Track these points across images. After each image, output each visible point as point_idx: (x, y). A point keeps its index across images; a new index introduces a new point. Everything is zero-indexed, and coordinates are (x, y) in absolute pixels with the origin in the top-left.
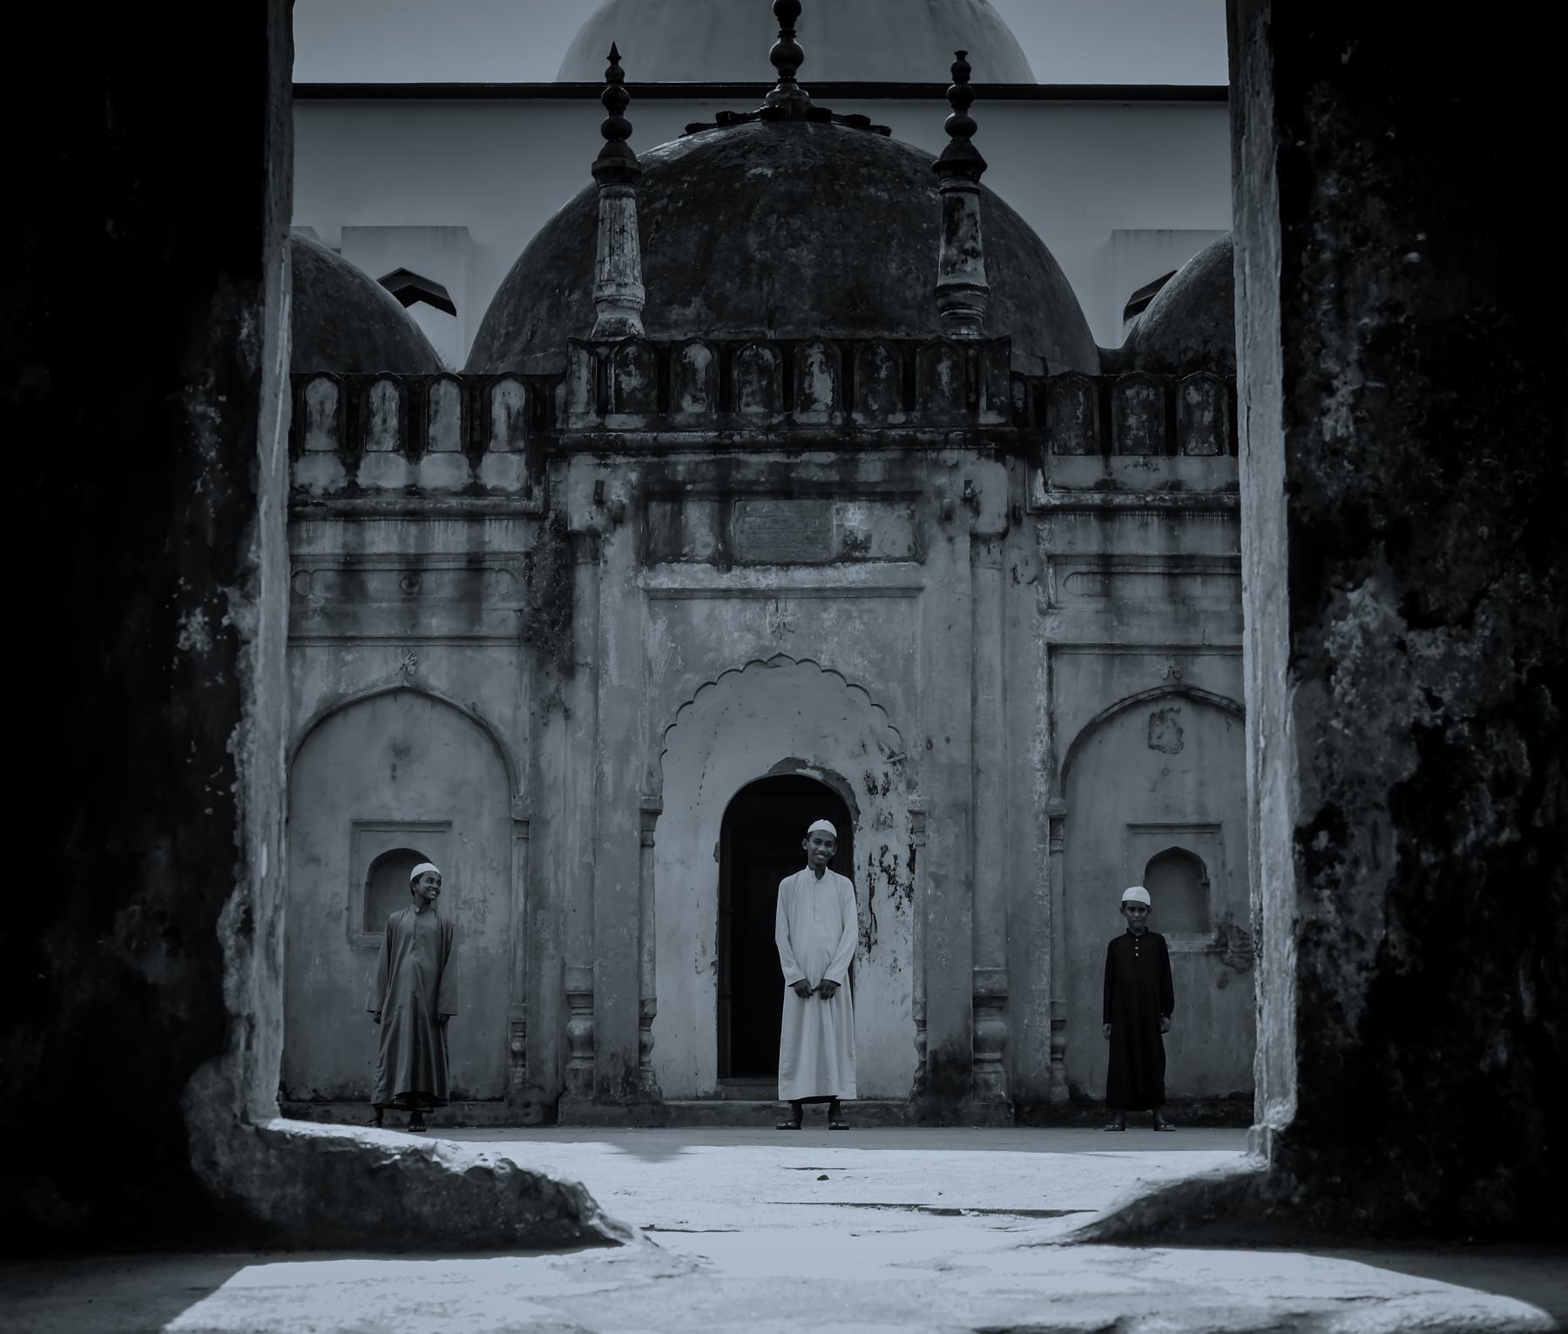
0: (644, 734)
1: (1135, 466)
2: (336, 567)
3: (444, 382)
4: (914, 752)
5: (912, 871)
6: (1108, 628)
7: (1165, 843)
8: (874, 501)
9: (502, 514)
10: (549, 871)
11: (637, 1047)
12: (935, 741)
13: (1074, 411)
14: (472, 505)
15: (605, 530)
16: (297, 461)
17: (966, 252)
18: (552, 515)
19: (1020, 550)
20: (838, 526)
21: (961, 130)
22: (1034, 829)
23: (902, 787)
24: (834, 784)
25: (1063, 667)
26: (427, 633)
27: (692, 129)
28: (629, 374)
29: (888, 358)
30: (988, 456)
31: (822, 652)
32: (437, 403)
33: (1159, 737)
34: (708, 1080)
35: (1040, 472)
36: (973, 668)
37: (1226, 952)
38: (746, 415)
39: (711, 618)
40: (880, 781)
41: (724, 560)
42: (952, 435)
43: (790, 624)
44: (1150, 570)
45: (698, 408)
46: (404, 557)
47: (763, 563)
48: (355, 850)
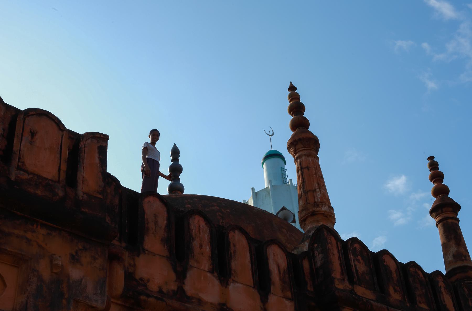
16: (138, 256)
28: (358, 261)
32: (234, 246)
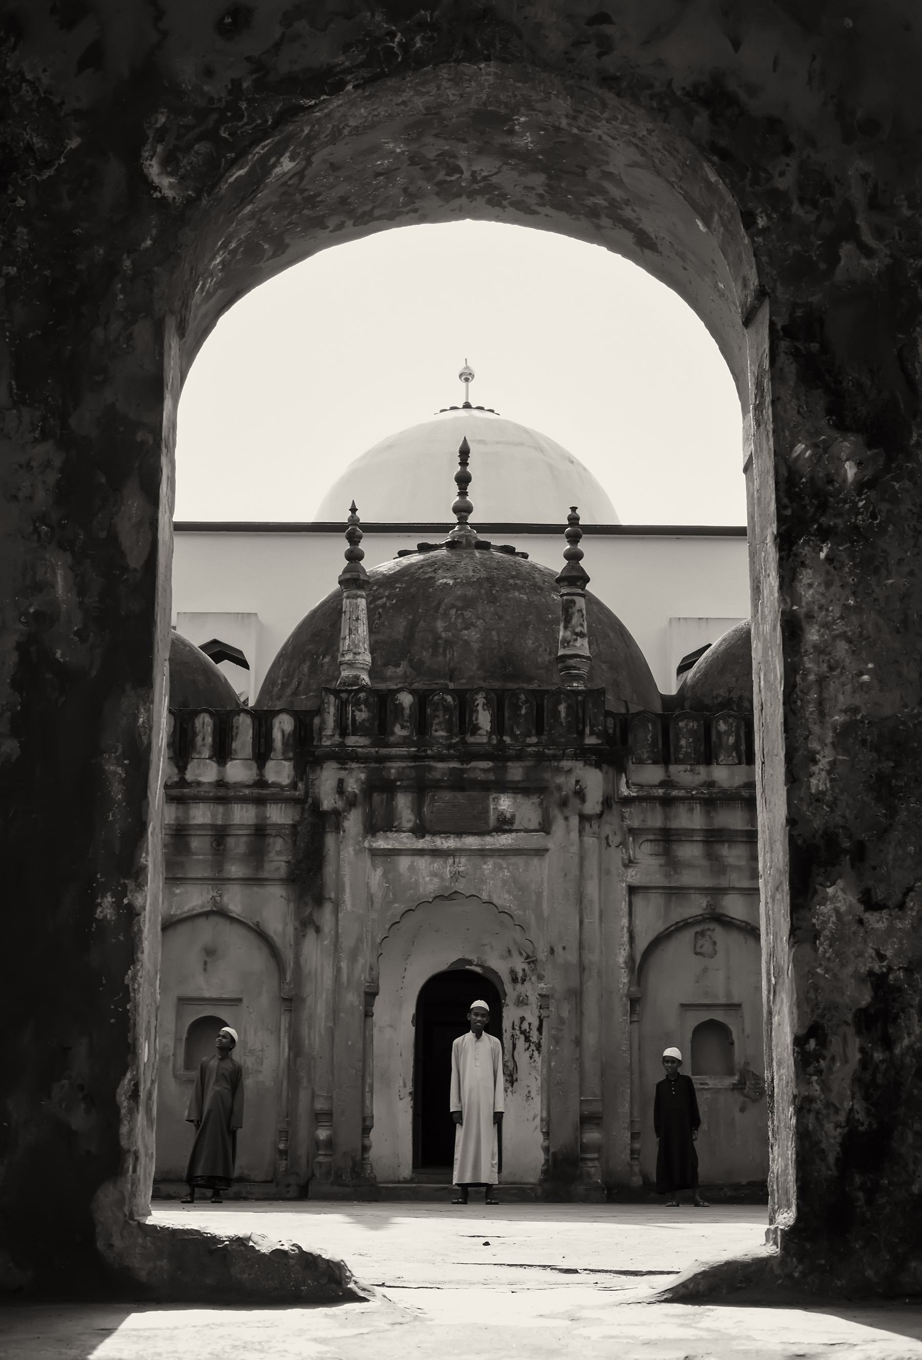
0: (367, 942)
1: (685, 771)
2: (171, 832)
3: (242, 714)
4: (542, 955)
5: (541, 1033)
6: (667, 876)
7: (705, 1016)
8: (515, 793)
9: (277, 800)
10: (305, 1031)
11: (360, 1147)
12: (555, 949)
13: (646, 735)
14: (259, 794)
15: (344, 811)
17: (577, 634)
18: (310, 800)
19: (611, 827)
20: (494, 809)
21: (574, 557)
22: (620, 1007)
23: (534, 978)
24: (489, 976)
25: (639, 902)
26: (229, 876)
27: (402, 554)
28: (361, 710)
29: (526, 702)
30: (591, 765)
31: (482, 890)
32: (237, 728)
33: (701, 947)
34: (406, 1169)
35: (624, 775)
36: (580, 899)
37: (744, 1088)
38: (435, 738)
39: (412, 868)
40: (520, 975)
41: (419, 831)
42: (568, 751)
43: (462, 872)
44: (695, 839)
45: (405, 733)
46: (213, 826)
47: (445, 833)
48: (179, 1016)
